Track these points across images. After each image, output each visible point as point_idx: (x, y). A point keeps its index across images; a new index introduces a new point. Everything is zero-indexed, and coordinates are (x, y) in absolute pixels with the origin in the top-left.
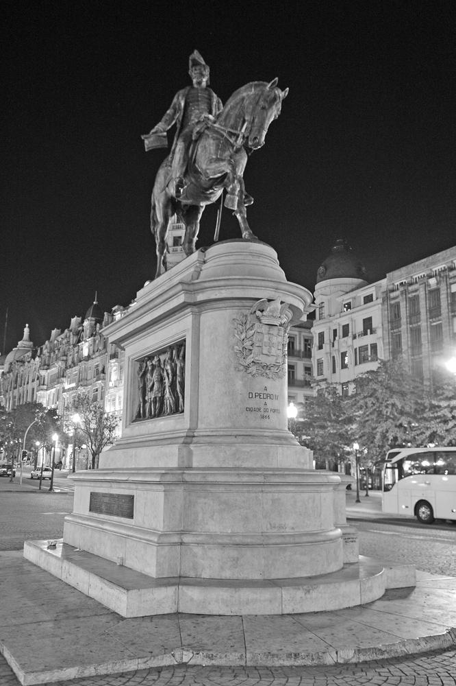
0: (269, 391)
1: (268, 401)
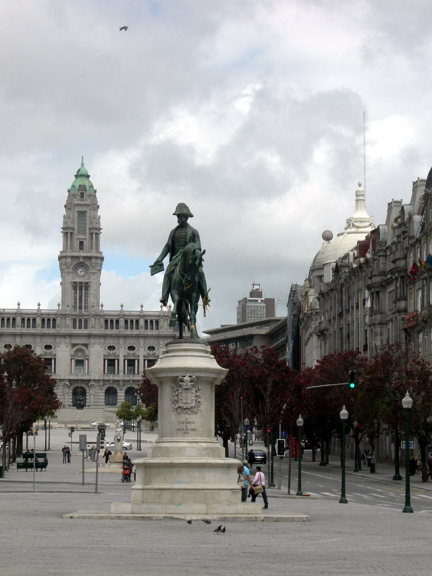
0: (188, 420)
1: (188, 425)
